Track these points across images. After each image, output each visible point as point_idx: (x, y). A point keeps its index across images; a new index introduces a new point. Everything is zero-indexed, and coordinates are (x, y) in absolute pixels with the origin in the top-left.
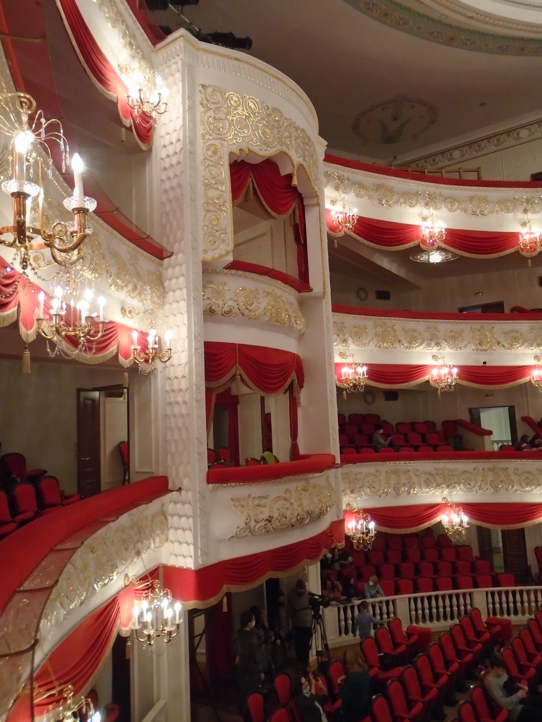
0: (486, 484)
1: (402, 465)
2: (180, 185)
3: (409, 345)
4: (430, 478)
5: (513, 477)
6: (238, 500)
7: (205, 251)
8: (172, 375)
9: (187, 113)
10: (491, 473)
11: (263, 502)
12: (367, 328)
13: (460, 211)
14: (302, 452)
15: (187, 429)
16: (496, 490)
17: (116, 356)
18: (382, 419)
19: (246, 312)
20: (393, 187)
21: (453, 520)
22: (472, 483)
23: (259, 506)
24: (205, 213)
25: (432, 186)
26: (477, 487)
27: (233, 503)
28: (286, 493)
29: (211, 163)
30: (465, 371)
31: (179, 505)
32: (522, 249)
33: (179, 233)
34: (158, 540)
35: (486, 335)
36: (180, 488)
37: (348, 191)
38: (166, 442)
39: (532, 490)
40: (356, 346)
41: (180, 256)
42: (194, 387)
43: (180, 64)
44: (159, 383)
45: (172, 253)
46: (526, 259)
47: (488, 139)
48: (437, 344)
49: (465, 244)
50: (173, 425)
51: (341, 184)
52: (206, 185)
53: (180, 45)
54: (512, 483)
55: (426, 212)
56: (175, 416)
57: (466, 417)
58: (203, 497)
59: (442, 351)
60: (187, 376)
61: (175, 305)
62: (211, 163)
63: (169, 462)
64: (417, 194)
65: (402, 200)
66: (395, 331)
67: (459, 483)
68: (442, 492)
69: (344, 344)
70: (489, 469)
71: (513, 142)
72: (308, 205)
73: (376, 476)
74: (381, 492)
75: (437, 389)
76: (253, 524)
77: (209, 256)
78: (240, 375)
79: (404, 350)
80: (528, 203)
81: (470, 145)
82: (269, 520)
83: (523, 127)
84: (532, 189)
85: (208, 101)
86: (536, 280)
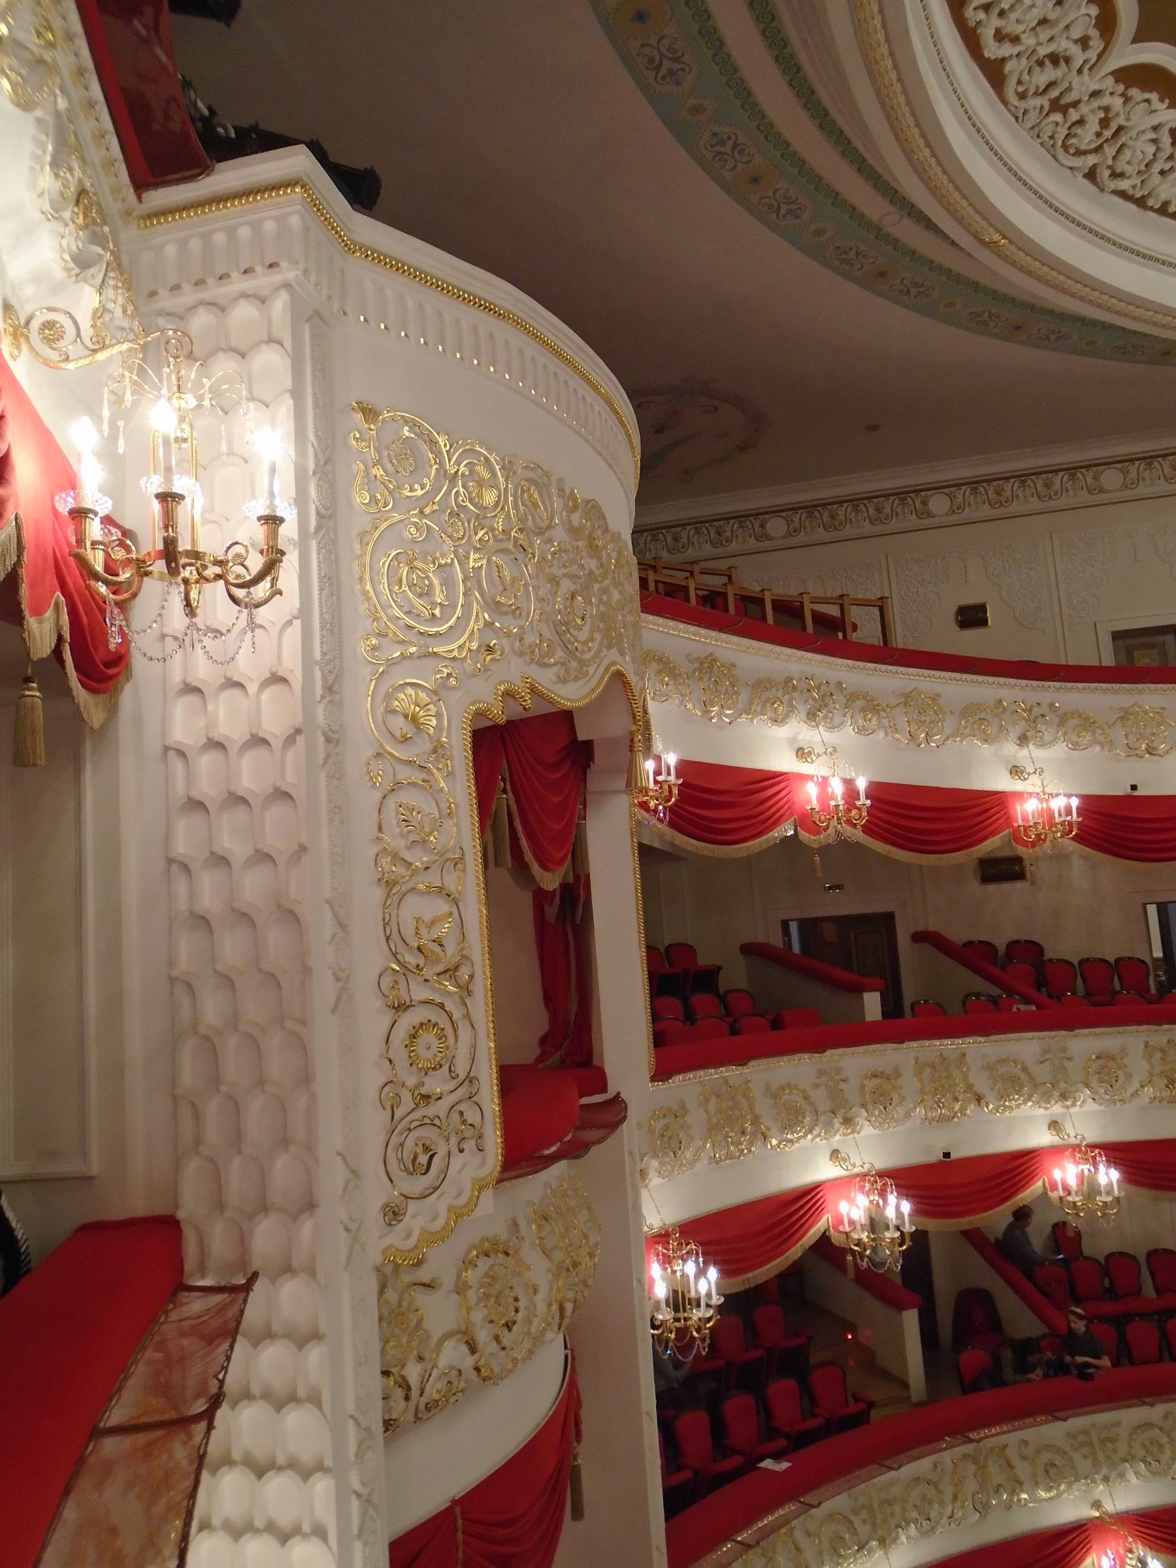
2: (290, 916)
7: (393, 1214)
9: (314, 544)
16: (983, 1509)
20: (734, 665)
24: (386, 1020)
26: (944, 1520)
29: (404, 774)
33: (282, 1166)
43: (280, 305)
47: (855, 501)
48: (848, 1121)
49: (888, 822)
53: (281, 220)
54: (1017, 1484)
71: (913, 521)
81: (810, 508)
83: (937, 488)
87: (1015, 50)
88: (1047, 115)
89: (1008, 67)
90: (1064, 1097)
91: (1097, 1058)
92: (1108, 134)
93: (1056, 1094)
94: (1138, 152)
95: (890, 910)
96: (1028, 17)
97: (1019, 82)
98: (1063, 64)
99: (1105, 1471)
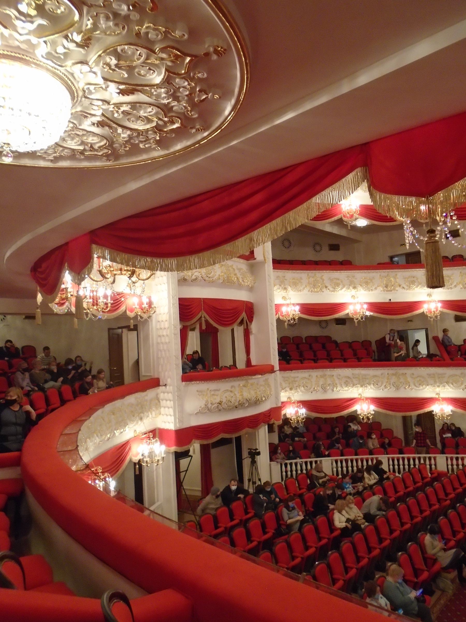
1: (328, 372)
3: (333, 289)
4: (348, 380)
6: (201, 391)
8: (160, 319)
10: (394, 377)
11: (217, 393)
15: (169, 351)
16: (398, 388)
17: (126, 311)
18: (333, 339)
19: (207, 279)
21: (365, 409)
26: (383, 387)
27: (197, 393)
31: (166, 394)
34: (154, 413)
35: (391, 280)
38: (158, 358)
39: (424, 389)
40: (294, 291)
44: (153, 324)
48: (354, 288)
50: (162, 348)
56: (162, 343)
58: (179, 390)
59: (357, 292)
61: (161, 278)
63: (160, 370)
66: (323, 280)
67: (369, 384)
69: (285, 291)
70: (393, 374)
73: (308, 379)
74: (312, 389)
78: (204, 317)
79: (330, 293)
82: (220, 403)
99: (438, 384)
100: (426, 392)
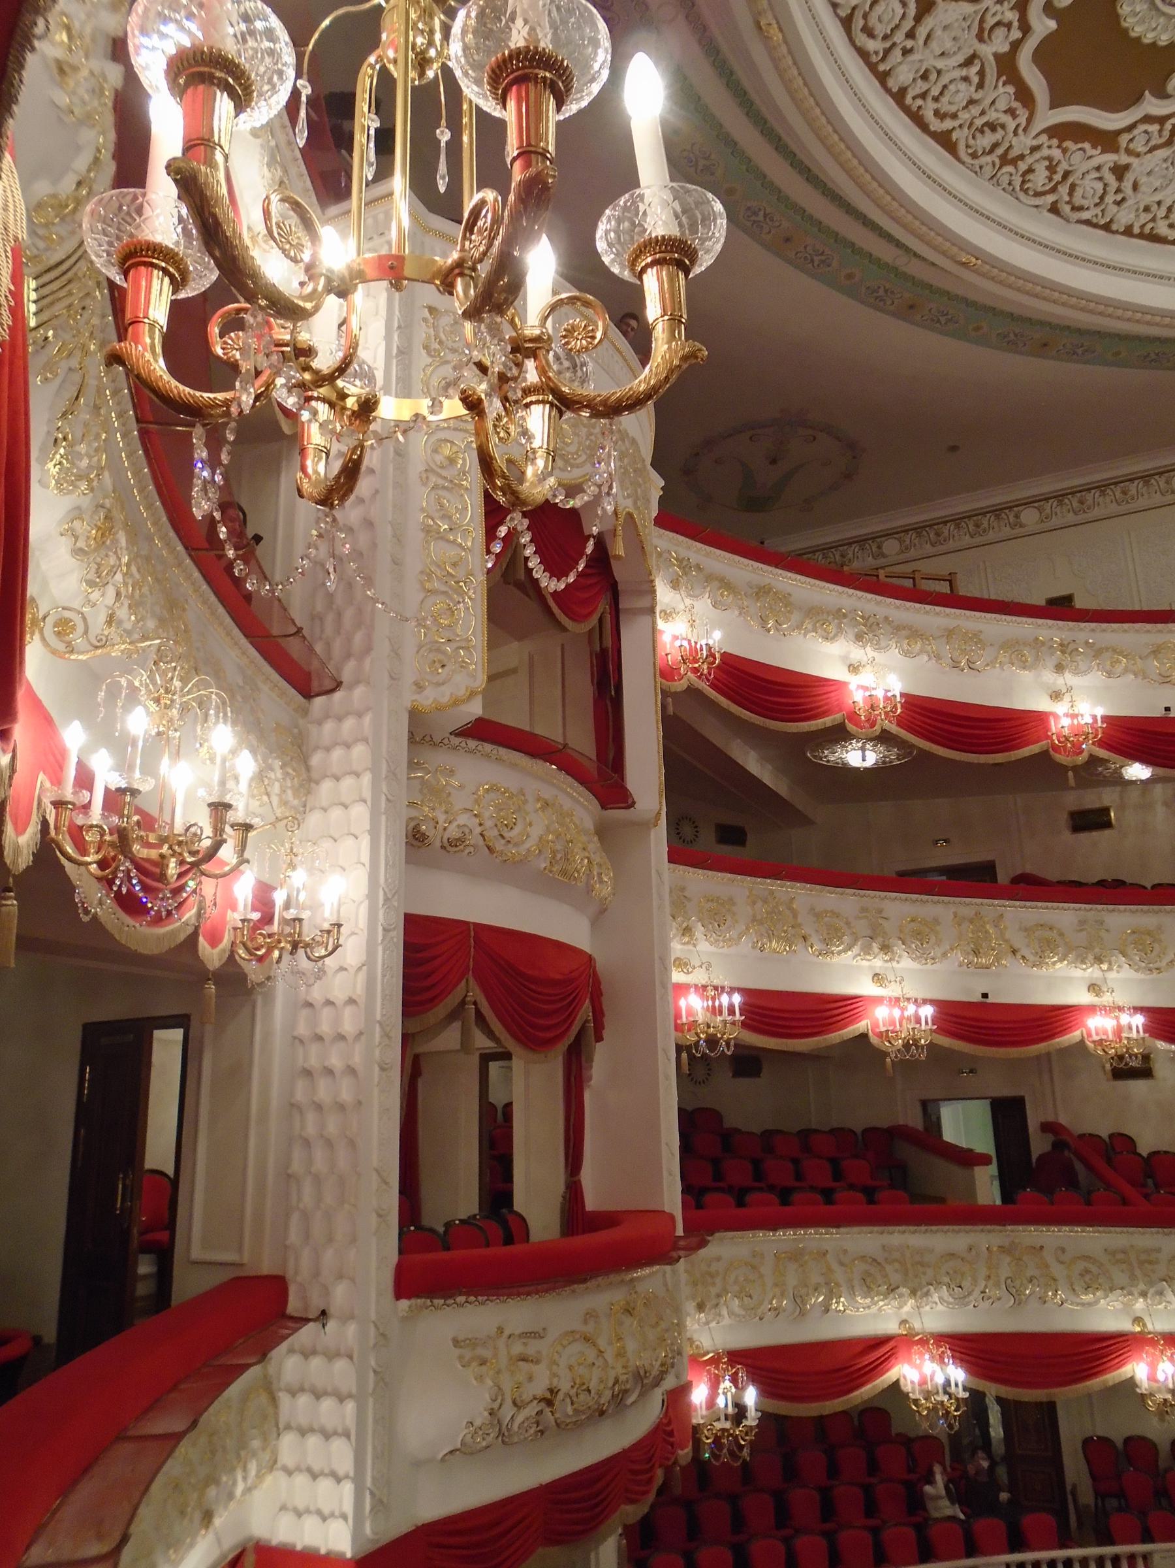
0: (997, 1285)
3: (824, 947)
5: (1057, 1270)
6: (472, 1343)
7: (419, 687)
9: (394, 361)
10: (1007, 1259)
12: (734, 904)
13: (926, 658)
14: (591, 1203)
15: (352, 1144)
19: (499, 845)
21: (928, 1376)
22: (966, 1284)
23: (524, 1359)
24: (422, 595)
25: (869, 601)
26: (977, 1293)
27: (457, 1351)
28: (586, 1322)
29: (440, 482)
30: (947, 1014)
31: (316, 1362)
32: (1056, 748)
33: (358, 638)
34: (253, 1467)
35: (987, 932)
36: (324, 1313)
37: (697, 592)
38: (288, 1177)
39: (1097, 1302)
41: (359, 691)
42: (378, 1029)
44: (277, 1016)
45: (338, 685)
46: (1064, 768)
47: (957, 520)
48: (885, 948)
50: (311, 1130)
51: (686, 576)
52: (427, 530)
55: (858, 653)
56: (319, 1107)
57: (914, 1119)
60: (362, 1001)
61: (336, 813)
62: (440, 482)
63: (294, 1237)
64: (839, 614)
65: (808, 624)
67: (936, 1283)
68: (900, 1307)
69: (686, 939)
71: (1007, 531)
72: (627, 610)
73: (754, 1267)
75: (886, 1054)
76: (508, 1411)
77: (428, 699)
78: (475, 1003)
79: (815, 959)
80: (1063, 652)
81: (919, 529)
83: (1028, 503)
84: (1071, 624)
85: (441, 343)
86: (1063, 819)
87: (956, 123)
88: (1000, 168)
89: (954, 136)
90: (1099, 960)
91: (1133, 932)
92: (1058, 177)
93: (1091, 957)
94: (1088, 188)
95: (990, 858)
96: (957, 99)
97: (968, 146)
98: (999, 129)
99: (1142, 1286)
100: (1106, 1314)
